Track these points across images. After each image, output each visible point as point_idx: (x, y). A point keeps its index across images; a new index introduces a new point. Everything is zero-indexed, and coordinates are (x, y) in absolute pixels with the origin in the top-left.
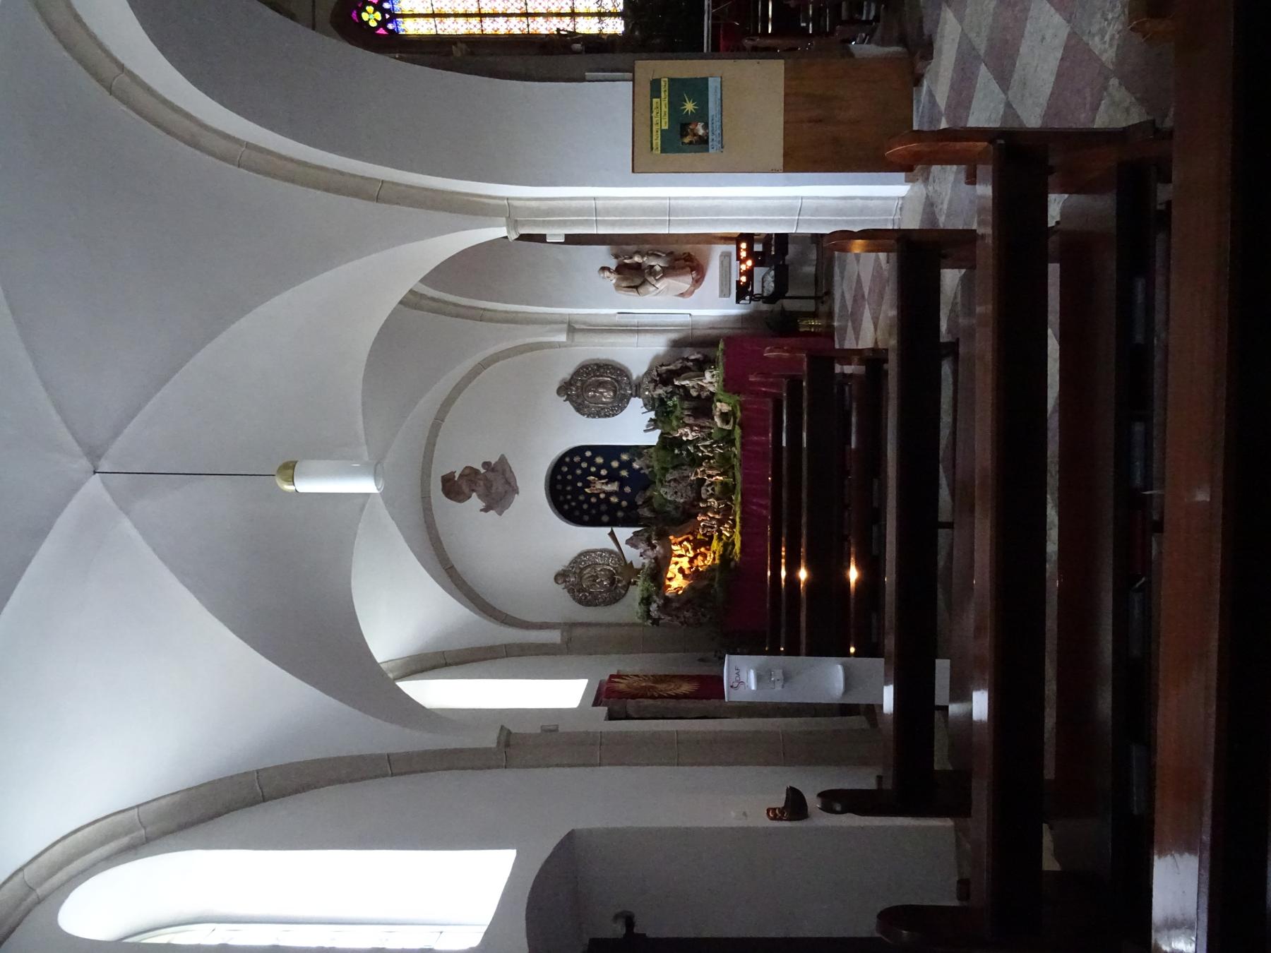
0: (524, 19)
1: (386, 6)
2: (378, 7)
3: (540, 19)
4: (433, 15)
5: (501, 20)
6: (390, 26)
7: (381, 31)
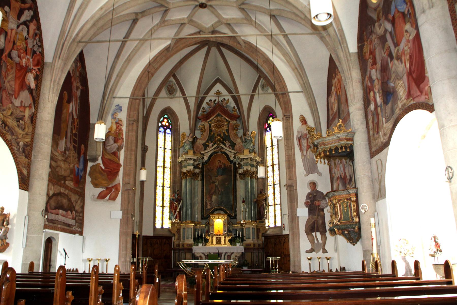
0: (272, 184)
4: (272, 146)
6: (268, 129)
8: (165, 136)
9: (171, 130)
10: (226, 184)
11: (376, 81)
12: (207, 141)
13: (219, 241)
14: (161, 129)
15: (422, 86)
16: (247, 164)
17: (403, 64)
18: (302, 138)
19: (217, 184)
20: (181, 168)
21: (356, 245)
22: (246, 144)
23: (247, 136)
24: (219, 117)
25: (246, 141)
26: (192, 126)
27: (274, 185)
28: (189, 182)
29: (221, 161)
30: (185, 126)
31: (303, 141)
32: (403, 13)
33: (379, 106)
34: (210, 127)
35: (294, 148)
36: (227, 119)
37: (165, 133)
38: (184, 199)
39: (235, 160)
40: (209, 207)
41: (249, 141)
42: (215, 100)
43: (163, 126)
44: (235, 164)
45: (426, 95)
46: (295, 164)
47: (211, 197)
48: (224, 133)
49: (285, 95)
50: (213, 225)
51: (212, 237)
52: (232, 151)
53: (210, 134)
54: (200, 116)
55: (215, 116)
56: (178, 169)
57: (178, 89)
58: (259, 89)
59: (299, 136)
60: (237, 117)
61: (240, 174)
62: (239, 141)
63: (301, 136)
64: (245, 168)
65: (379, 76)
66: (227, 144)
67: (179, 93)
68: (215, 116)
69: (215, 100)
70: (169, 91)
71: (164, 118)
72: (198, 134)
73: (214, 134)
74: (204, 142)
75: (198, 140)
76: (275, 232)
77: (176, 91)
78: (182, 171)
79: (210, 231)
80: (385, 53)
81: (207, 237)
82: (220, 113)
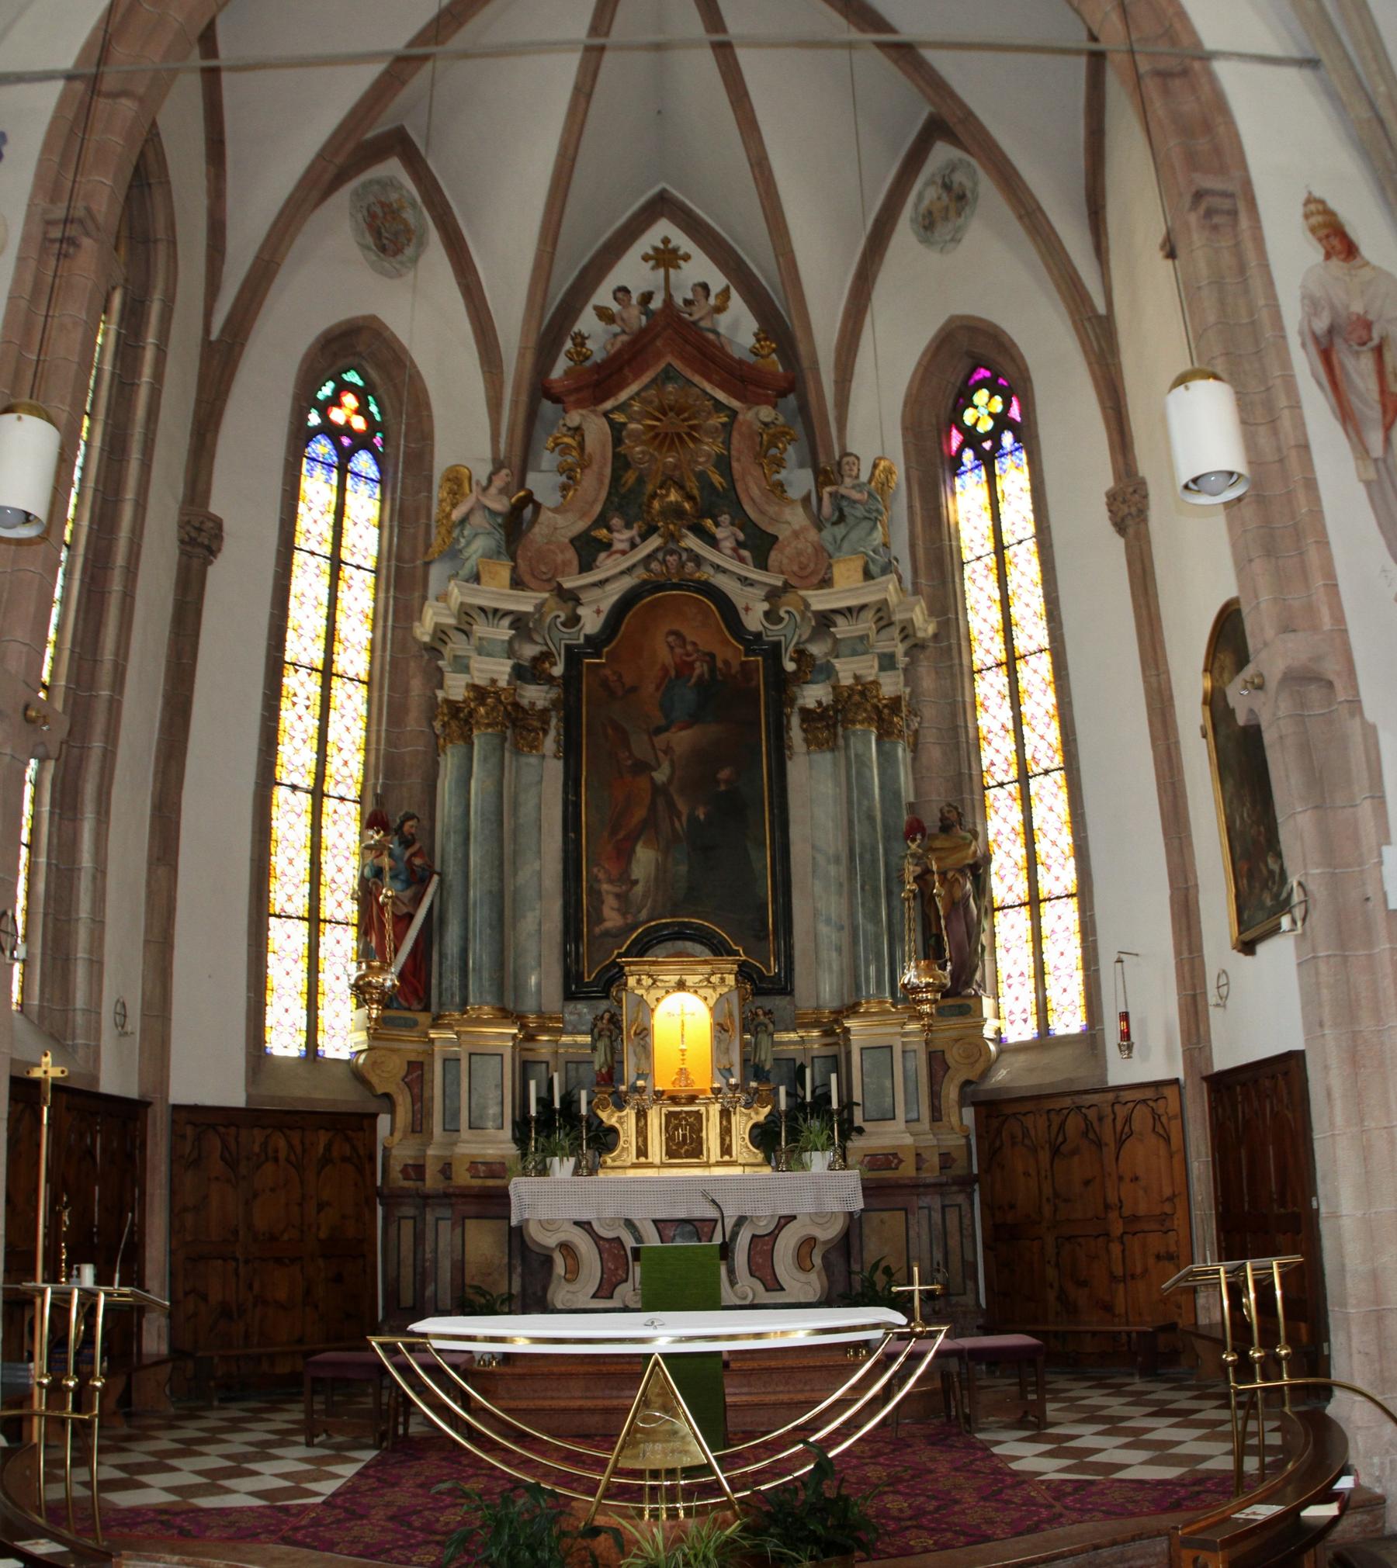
0: (1013, 773)
1: (1007, 439)
2: (1002, 421)
3: (1016, 817)
4: (1000, 548)
5: (1006, 715)
6: (968, 456)
7: (956, 439)
8: (342, 489)
9: (378, 459)
10: (724, 774)
12: (602, 521)
13: (685, 1142)
14: (322, 447)
16: (859, 646)
18: (1339, 343)
19: (660, 776)
20: (437, 679)
22: (840, 531)
23: (848, 481)
24: (670, 388)
25: (841, 518)
26: (510, 444)
27: (1024, 778)
28: (485, 759)
29: (690, 638)
30: (464, 431)
31: (1350, 363)
34: (617, 441)
35: (1296, 406)
36: (721, 396)
37: (343, 471)
38: (452, 870)
39: (774, 633)
40: (612, 919)
41: (860, 512)
42: (647, 297)
43: (332, 431)
44: (774, 652)
46: (1317, 513)
47: (624, 855)
48: (702, 477)
49: (1176, 84)
50: (644, 1033)
51: (641, 1115)
52: (755, 575)
53: (616, 479)
54: (551, 383)
55: (646, 378)
56: (416, 685)
57: (434, 236)
58: (904, 233)
59: (1321, 325)
60: (784, 380)
61: (806, 714)
62: (797, 517)
63: (1331, 331)
64: (846, 671)
66: (720, 533)
67: (435, 254)
68: (646, 378)
69: (647, 297)
70: (377, 234)
71: (342, 387)
72: (543, 483)
73: (641, 480)
74: (581, 526)
75: (545, 516)
76: (1053, 1073)
77: (421, 245)
78: (440, 694)
79: (629, 1071)
81: (608, 1117)
82: (678, 365)
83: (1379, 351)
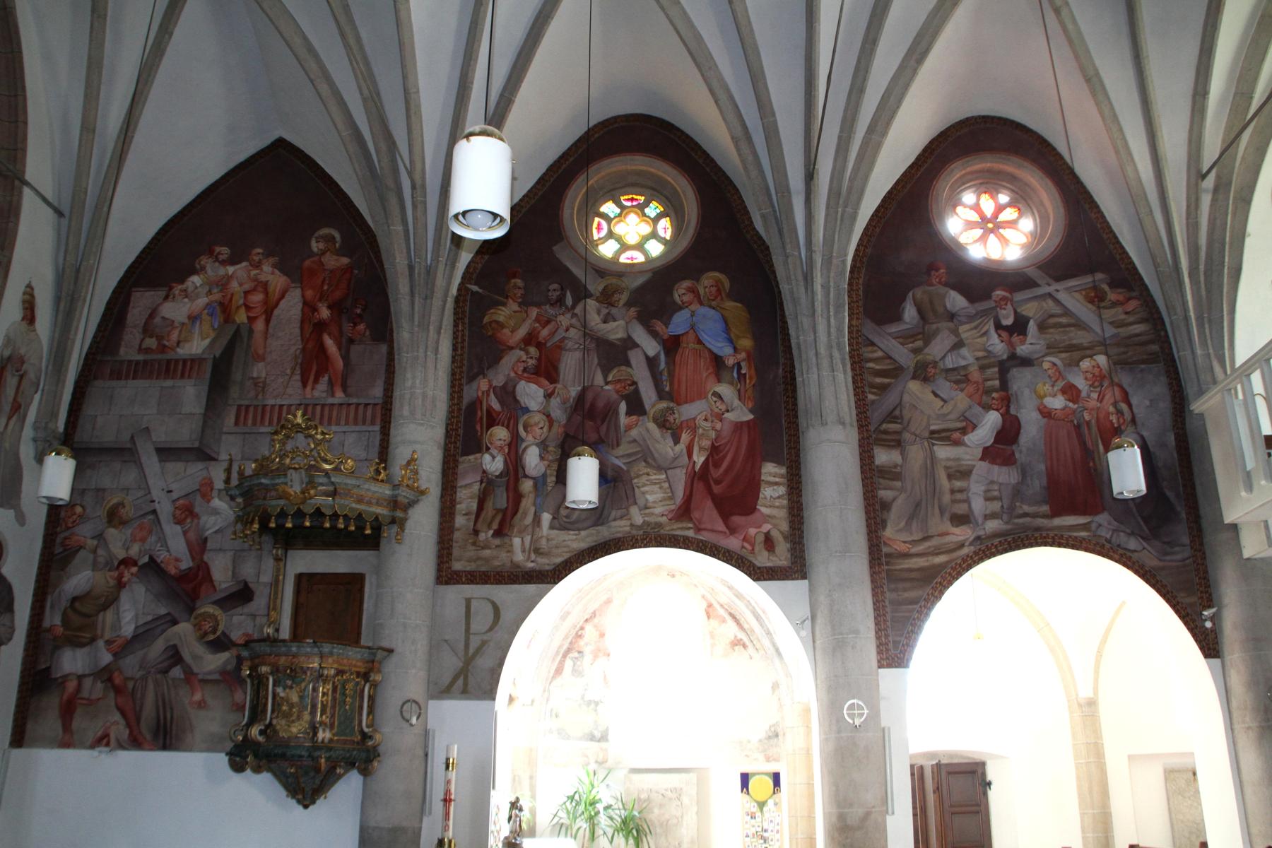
11: (538, 418)
15: (737, 519)
17: (681, 447)
21: (311, 807)
32: (717, 361)
33: (526, 476)
45: (744, 539)
65: (558, 414)
80: (607, 383)
83: (21, 377)
